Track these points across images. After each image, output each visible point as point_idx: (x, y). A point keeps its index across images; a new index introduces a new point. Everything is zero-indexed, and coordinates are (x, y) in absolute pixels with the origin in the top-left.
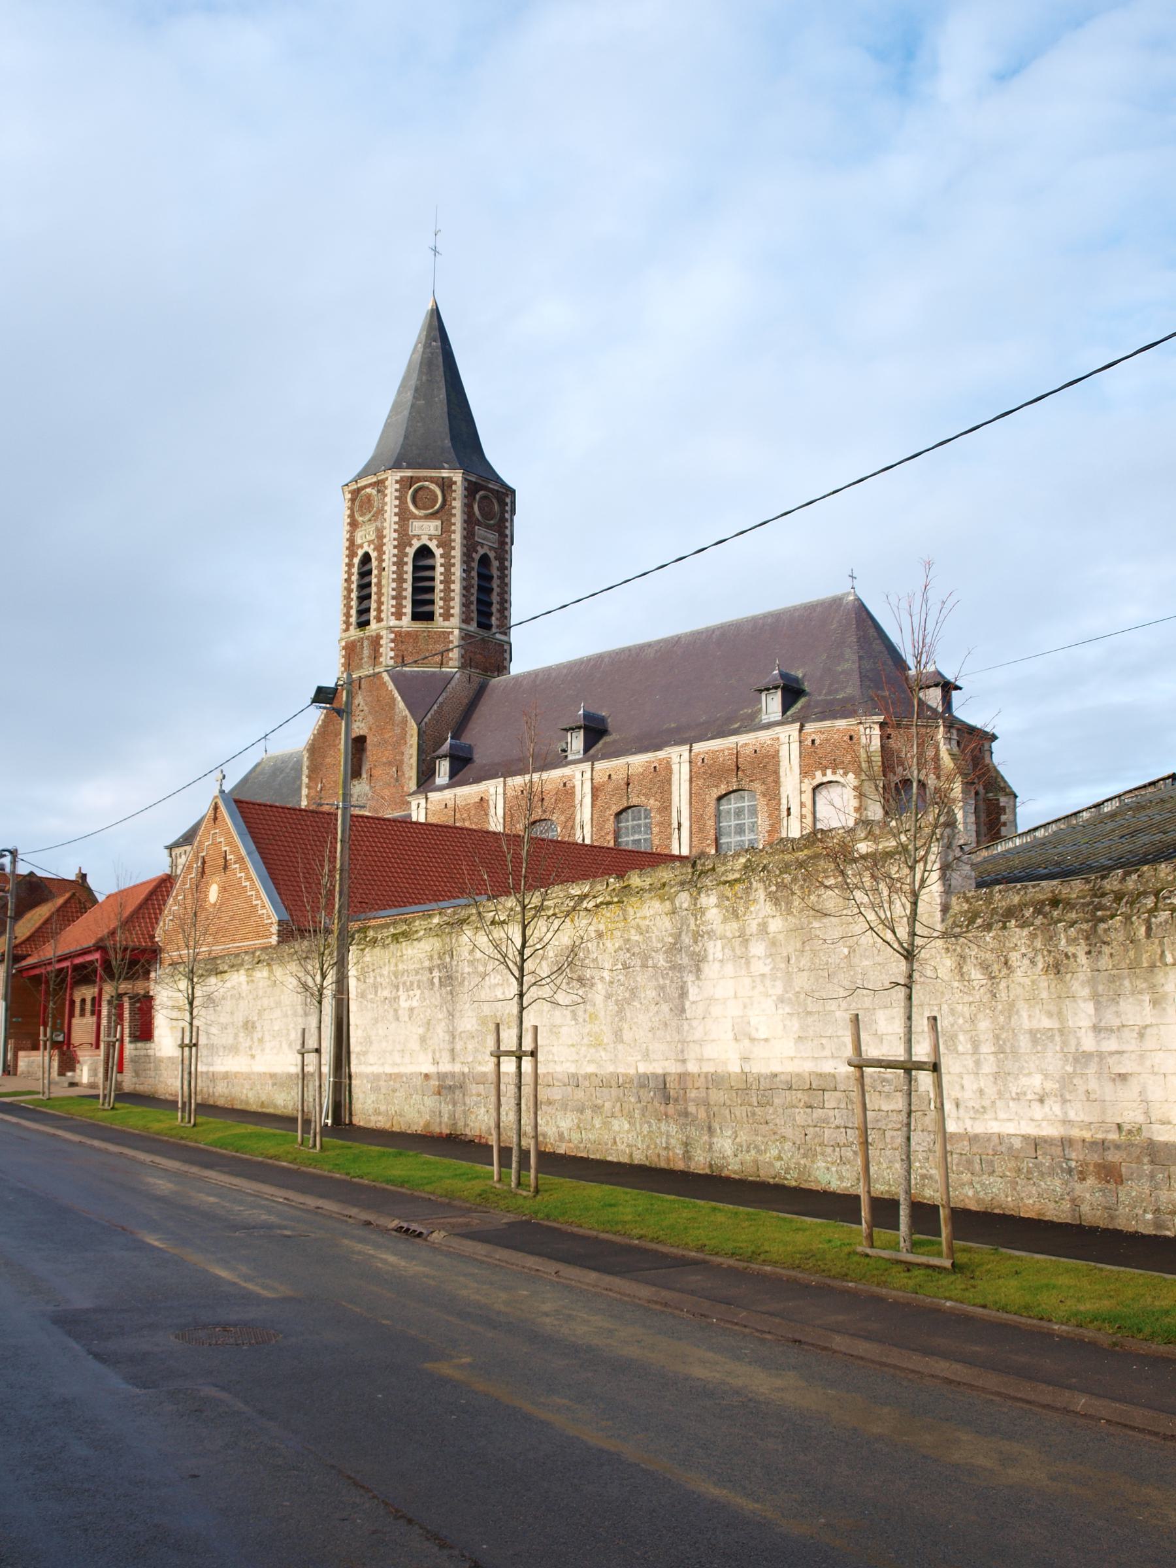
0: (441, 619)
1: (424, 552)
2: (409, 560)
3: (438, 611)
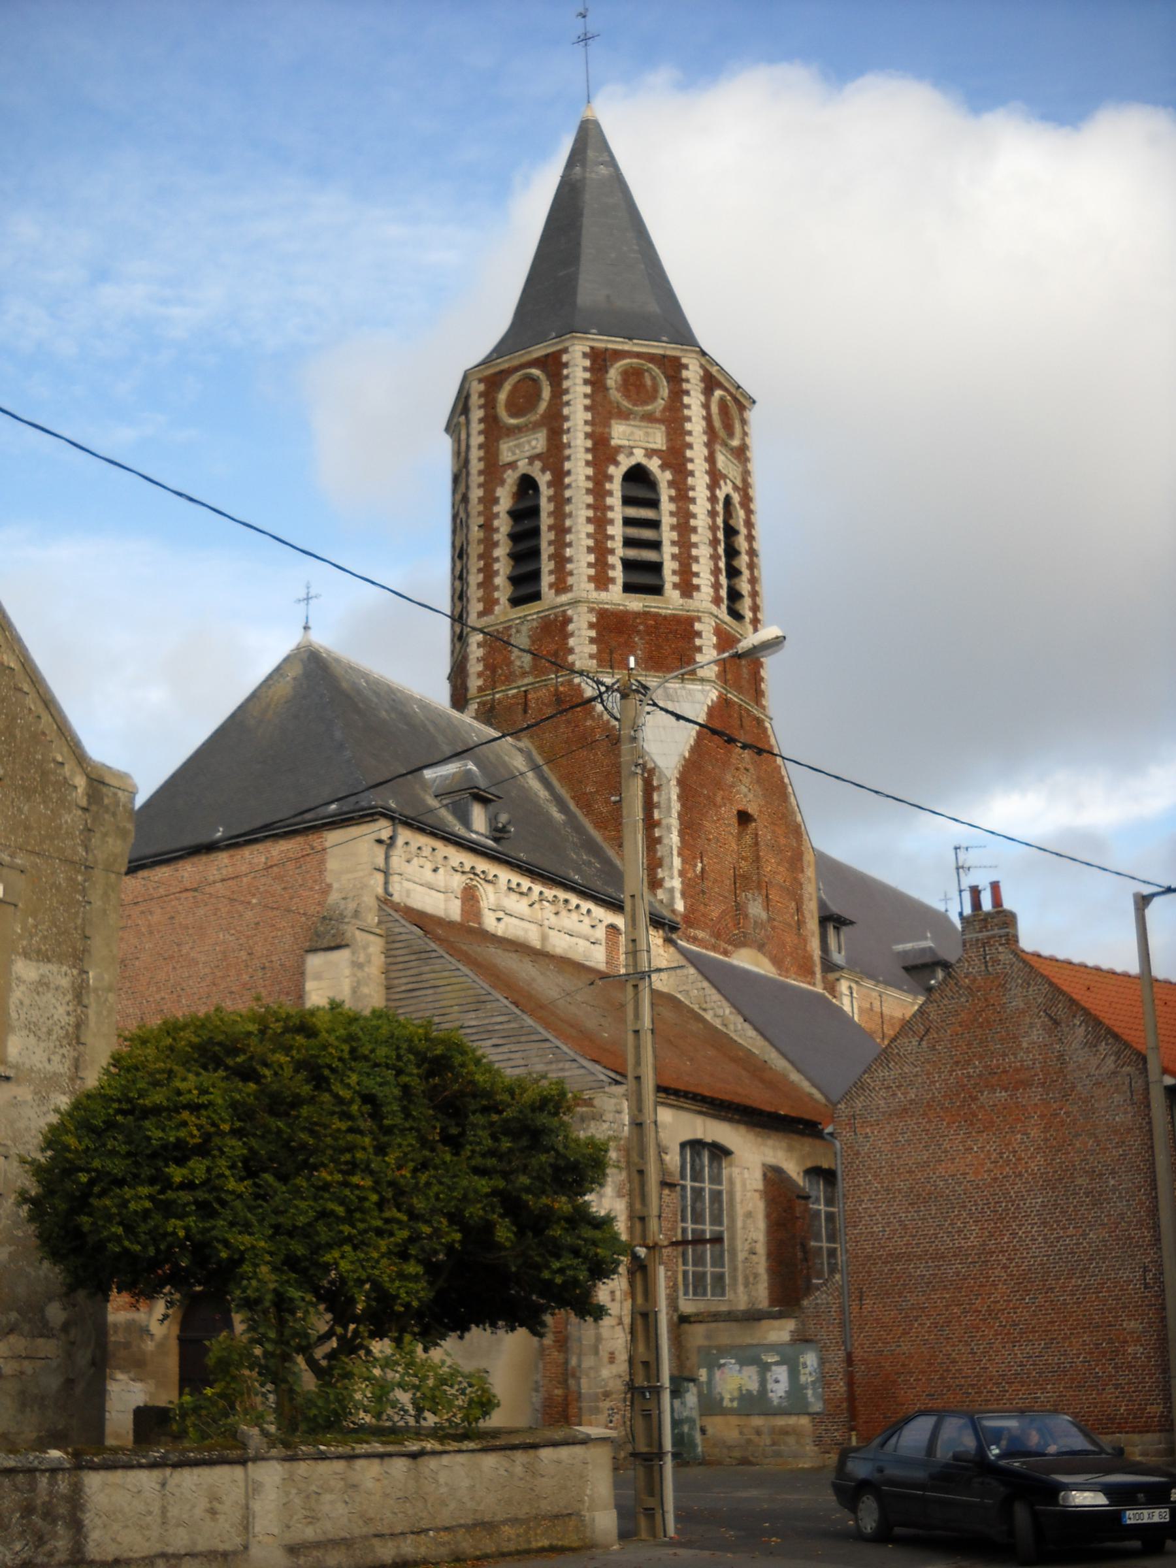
0: (677, 593)
1: (638, 476)
2: (616, 487)
3: (669, 577)
